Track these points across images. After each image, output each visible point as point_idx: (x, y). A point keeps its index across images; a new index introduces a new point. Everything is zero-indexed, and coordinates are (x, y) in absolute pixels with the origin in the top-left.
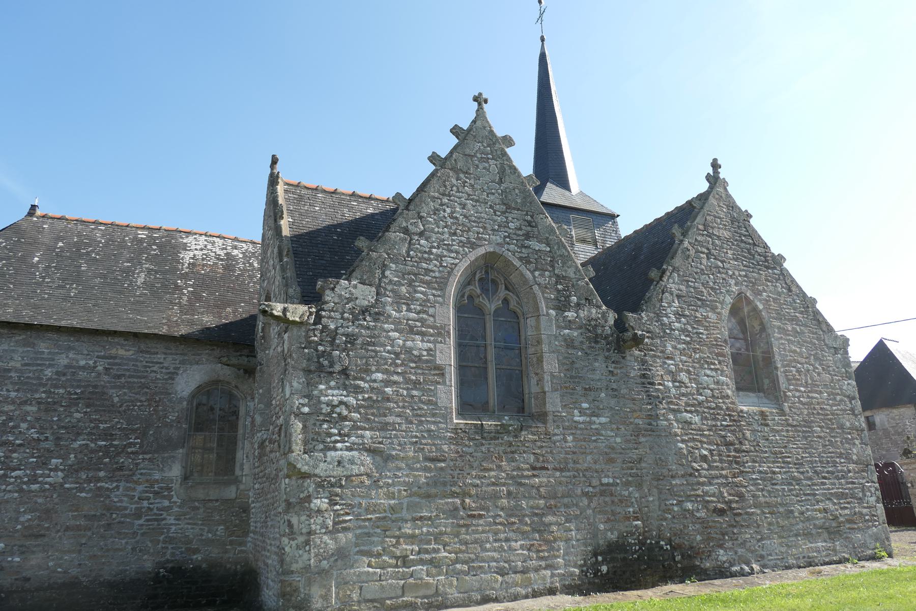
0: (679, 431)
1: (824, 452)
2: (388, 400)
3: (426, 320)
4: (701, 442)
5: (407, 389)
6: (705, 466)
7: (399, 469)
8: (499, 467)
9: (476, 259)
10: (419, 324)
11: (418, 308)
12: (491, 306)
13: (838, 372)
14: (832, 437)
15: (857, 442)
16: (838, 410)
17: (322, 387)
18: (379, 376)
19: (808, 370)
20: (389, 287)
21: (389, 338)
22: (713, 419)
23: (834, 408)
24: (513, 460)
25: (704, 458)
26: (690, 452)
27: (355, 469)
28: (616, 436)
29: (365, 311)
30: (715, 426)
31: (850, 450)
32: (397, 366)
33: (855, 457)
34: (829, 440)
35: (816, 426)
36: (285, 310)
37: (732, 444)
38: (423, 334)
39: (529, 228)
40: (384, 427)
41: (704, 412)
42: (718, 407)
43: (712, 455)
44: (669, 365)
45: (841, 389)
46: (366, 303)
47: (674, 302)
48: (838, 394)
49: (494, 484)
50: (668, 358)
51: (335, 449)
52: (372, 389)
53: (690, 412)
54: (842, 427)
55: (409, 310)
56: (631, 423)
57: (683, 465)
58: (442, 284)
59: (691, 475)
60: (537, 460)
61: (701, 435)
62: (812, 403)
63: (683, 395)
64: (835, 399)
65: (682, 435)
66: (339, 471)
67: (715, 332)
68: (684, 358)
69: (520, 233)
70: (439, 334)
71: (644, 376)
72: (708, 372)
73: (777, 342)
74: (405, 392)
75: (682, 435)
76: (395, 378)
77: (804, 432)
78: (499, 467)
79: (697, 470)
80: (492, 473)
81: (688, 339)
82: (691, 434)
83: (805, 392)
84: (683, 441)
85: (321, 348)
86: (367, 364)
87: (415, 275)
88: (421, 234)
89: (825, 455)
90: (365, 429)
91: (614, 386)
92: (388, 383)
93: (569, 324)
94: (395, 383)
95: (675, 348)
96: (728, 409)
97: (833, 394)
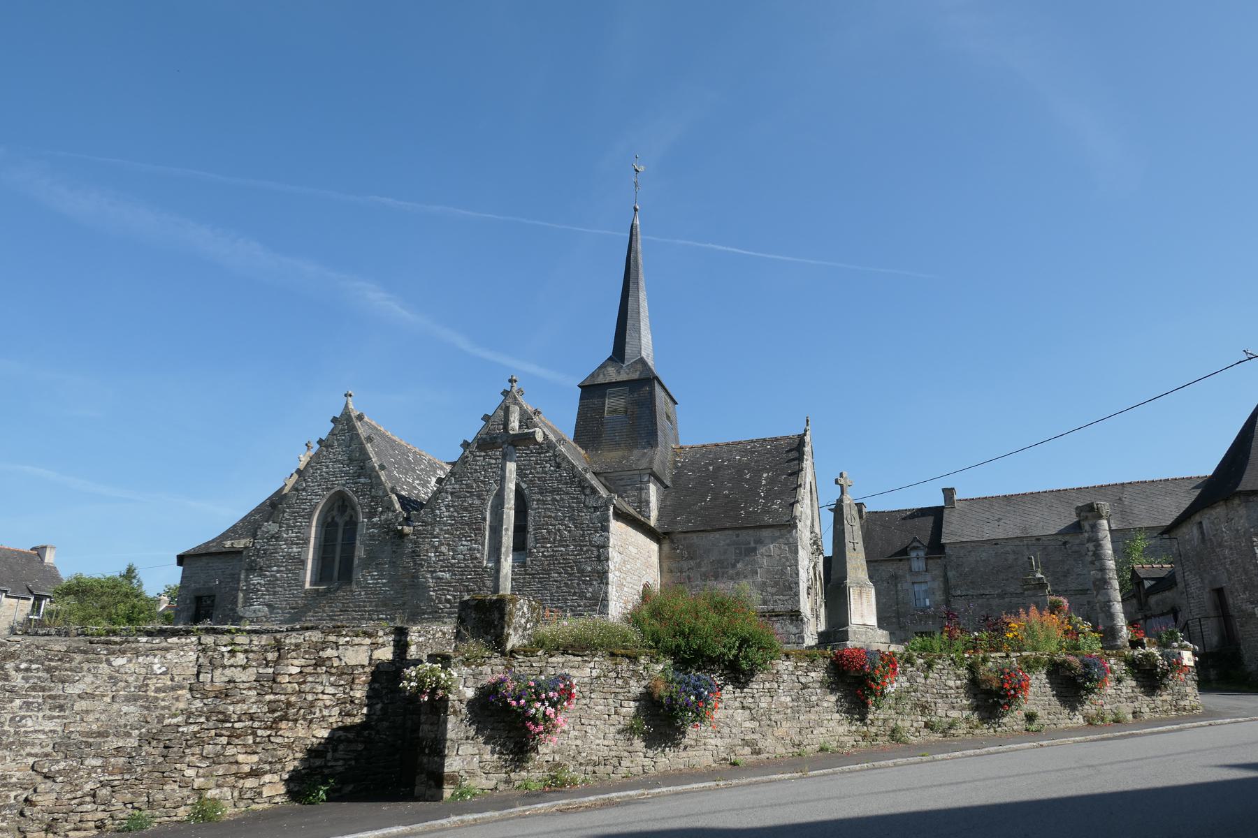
0: (431, 585)
1: (557, 592)
2: (277, 580)
3: (299, 536)
4: (448, 591)
5: (287, 574)
6: (448, 605)
7: (278, 613)
8: (324, 611)
9: (330, 497)
10: (295, 539)
11: (297, 531)
12: (340, 521)
13: (591, 527)
14: (569, 580)
15: (595, 583)
17: (251, 576)
18: (275, 568)
19: (559, 530)
20: (285, 522)
21: (281, 548)
22: (461, 575)
24: (331, 607)
25: (448, 601)
26: (437, 597)
27: (260, 614)
28: (391, 590)
29: (273, 537)
30: (463, 579)
32: (283, 562)
33: (589, 595)
34: (565, 583)
36: (232, 544)
37: (473, 590)
38: (297, 544)
39: (361, 471)
40: (275, 593)
41: (455, 571)
43: (455, 599)
44: (434, 542)
45: (590, 541)
46: (274, 532)
47: (447, 498)
48: (586, 545)
49: (320, 620)
50: (435, 538)
51: (254, 605)
52: (272, 575)
53: (444, 571)
54: (582, 571)
55: (292, 533)
56: (401, 582)
57: (431, 606)
58: (310, 515)
59: (436, 612)
60: (343, 606)
61: (449, 586)
63: (440, 560)
64: (581, 550)
65: (434, 587)
66: (254, 615)
67: (476, 513)
68: (447, 536)
69: (356, 475)
70: (305, 543)
71: (414, 552)
72: (464, 543)
73: (533, 513)
74: (285, 576)
75: (434, 587)
76: (282, 569)
77: (541, 578)
78: (324, 611)
79: (441, 609)
80: (320, 614)
81: (453, 522)
82: (441, 586)
83: (551, 547)
84: (434, 591)
85: (253, 558)
86: (270, 563)
87: (297, 513)
88: (304, 490)
89: (557, 595)
90: (266, 595)
91: (394, 560)
92: (278, 572)
93: (374, 525)
94: (282, 571)
95: (441, 530)
96: (474, 567)
97: (580, 546)
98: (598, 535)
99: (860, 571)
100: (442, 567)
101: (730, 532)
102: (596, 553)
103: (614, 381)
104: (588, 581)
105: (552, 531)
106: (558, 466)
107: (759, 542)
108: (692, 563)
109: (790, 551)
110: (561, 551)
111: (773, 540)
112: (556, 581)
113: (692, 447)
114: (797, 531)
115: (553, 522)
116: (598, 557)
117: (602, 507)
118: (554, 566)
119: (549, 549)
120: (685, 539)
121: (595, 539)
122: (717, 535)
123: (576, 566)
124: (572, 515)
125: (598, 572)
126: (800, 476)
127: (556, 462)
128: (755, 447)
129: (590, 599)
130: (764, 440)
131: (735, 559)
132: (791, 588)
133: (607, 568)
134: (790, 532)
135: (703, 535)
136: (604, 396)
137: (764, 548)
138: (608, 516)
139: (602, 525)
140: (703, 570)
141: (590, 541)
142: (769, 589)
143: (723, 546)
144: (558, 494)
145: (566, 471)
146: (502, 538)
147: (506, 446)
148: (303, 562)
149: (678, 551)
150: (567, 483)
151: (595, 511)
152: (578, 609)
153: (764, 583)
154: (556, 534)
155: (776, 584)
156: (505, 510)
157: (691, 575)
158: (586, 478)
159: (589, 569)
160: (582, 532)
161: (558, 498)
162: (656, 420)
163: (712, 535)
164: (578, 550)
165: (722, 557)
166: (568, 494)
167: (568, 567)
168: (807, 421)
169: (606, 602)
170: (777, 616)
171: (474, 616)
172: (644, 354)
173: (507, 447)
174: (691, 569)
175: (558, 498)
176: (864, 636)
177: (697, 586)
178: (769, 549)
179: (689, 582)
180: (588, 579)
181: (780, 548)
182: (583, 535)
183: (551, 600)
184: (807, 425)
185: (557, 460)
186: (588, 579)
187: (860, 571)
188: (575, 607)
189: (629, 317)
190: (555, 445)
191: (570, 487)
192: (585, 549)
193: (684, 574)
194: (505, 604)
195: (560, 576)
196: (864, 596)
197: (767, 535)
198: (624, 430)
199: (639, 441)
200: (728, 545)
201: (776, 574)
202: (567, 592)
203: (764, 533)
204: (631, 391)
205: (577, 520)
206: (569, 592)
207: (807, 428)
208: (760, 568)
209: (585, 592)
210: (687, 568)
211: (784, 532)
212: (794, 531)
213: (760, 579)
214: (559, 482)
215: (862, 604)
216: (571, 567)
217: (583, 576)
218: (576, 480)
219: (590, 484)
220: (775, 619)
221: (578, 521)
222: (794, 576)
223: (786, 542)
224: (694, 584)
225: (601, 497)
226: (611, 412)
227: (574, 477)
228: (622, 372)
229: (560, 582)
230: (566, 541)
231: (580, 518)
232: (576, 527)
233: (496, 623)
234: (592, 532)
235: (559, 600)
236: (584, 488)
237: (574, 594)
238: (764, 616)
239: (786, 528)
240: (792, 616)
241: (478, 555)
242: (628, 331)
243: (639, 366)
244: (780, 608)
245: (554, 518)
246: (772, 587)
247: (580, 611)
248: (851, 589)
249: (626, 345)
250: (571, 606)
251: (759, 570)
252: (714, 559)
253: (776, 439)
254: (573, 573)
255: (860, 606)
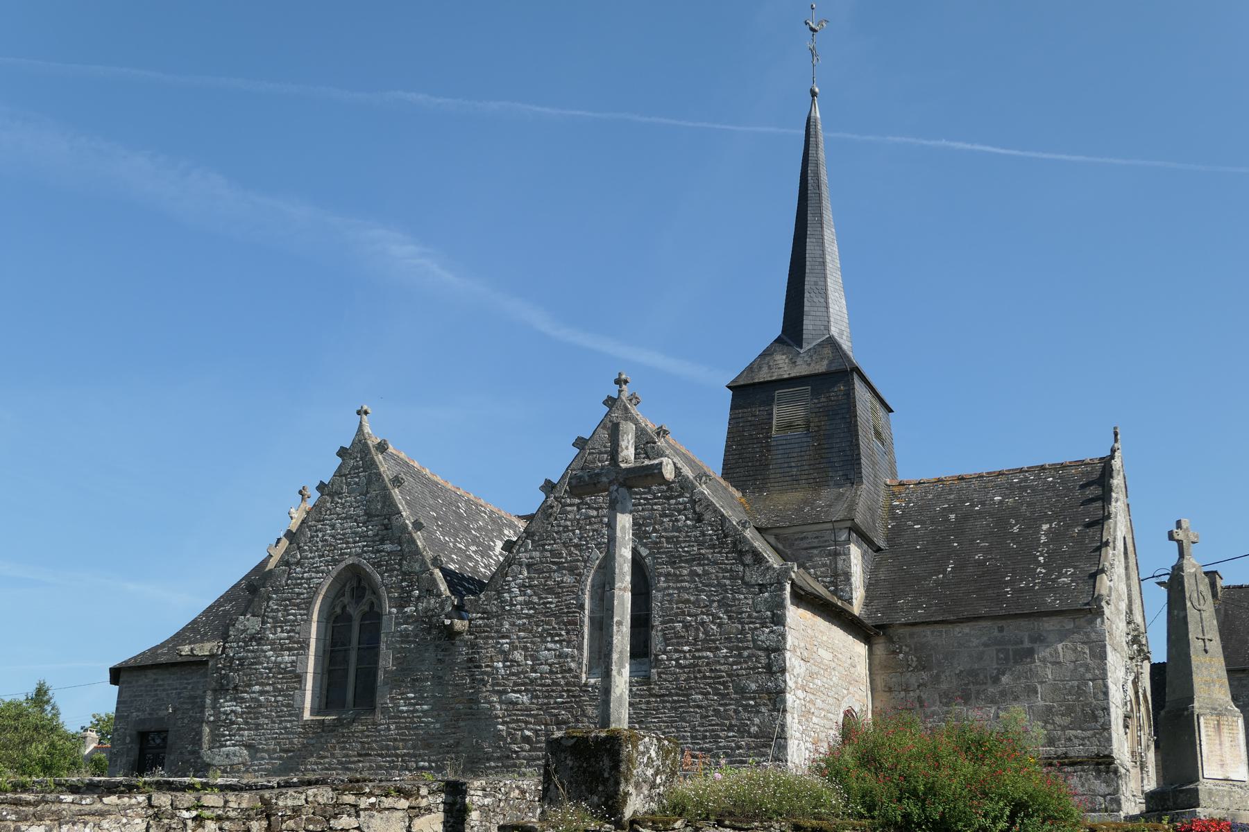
0: (499, 713)
1: (702, 725)
2: (261, 706)
3: (293, 637)
4: (527, 723)
5: (275, 696)
6: (527, 747)
7: (263, 759)
8: (333, 756)
9: (339, 574)
10: (287, 641)
11: (288, 628)
12: (355, 612)
13: (756, 618)
14: (721, 705)
15: (763, 709)
16: (741, 669)
17: (222, 701)
18: (257, 688)
19: (703, 623)
20: (271, 614)
21: (265, 656)
22: (546, 697)
23: (735, 667)
24: (343, 748)
25: (526, 739)
26: (509, 734)
27: (236, 760)
28: (437, 722)
29: (253, 638)
30: (549, 704)
31: (749, 720)
32: (268, 678)
33: (754, 729)
34: (714, 710)
35: (696, 693)
36: (192, 650)
37: (565, 722)
38: (289, 649)
39: (385, 532)
40: (258, 727)
41: (536, 691)
42: (555, 684)
43: (537, 735)
44: (502, 644)
45: (754, 641)
46: (254, 631)
47: (521, 573)
48: (748, 648)
49: (327, 769)
50: (503, 637)
51: (225, 746)
52: (252, 698)
53: (519, 692)
54: (742, 691)
55: (282, 631)
56: (452, 709)
57: (500, 747)
58: (309, 604)
59: (508, 757)
60: (363, 748)
61: (527, 715)
62: (697, 665)
63: (513, 674)
64: (740, 655)
65: (504, 716)
66: (226, 762)
67: (568, 598)
68: (522, 634)
69: (377, 538)
70: (302, 648)
71: (470, 660)
72: (549, 645)
73: (659, 595)
74: (273, 699)
75: (504, 716)
76: (268, 688)
77: (674, 702)
78: (333, 756)
79: (516, 752)
80: (327, 760)
81: (532, 612)
82: (515, 715)
83: (690, 651)
84: (503, 723)
85: (223, 672)
86: (250, 680)
87: (289, 600)
88: (298, 563)
89: (702, 729)
90: (245, 730)
91: (440, 674)
92: (262, 693)
93: (407, 619)
94: (268, 692)
95: (513, 624)
96: (567, 684)
97: (738, 648)
98: (767, 630)
99: (1217, 686)
100: (516, 684)
101: (989, 623)
102: (764, 661)
103: (786, 376)
104: (752, 706)
105: (691, 625)
106: (699, 518)
107: (1039, 639)
108: (924, 675)
109: (1093, 655)
110: (707, 657)
111: (1063, 636)
112: (699, 707)
113: (920, 483)
114: (1103, 621)
115: (693, 611)
116: (768, 667)
117: (772, 585)
118: (696, 683)
119: (687, 655)
120: (911, 635)
121: (762, 638)
122: (966, 629)
123: (732, 681)
124: (723, 598)
125: (769, 692)
126: (1105, 527)
127: (695, 512)
128: (1026, 479)
129: (756, 736)
130: (1042, 468)
131: (999, 669)
132: (1095, 718)
133: (783, 686)
134: (1092, 621)
135: (943, 628)
136: (769, 402)
137: (1048, 650)
138: (783, 600)
139: (774, 615)
140: (944, 686)
141: (754, 641)
142: (1057, 719)
143: (977, 647)
144: (699, 565)
145: (712, 525)
146: (612, 637)
147: (615, 487)
148: (300, 678)
149: (901, 656)
150: (713, 547)
151: (761, 592)
152: (737, 752)
153: (1049, 709)
154: (697, 629)
155: (1070, 710)
156: (617, 592)
157: (924, 696)
158: (744, 537)
159: (753, 686)
160: (740, 626)
161: (699, 570)
162: (857, 440)
163: (957, 629)
164: (735, 656)
165: (976, 666)
166: (715, 563)
167: (719, 683)
168: (1116, 434)
169: (782, 741)
170: (1073, 764)
171: (570, 763)
172: (834, 331)
173: (617, 490)
174: (924, 685)
175: (699, 570)
176: (1226, 799)
177: (933, 714)
178: (1056, 651)
179: (921, 707)
180: (752, 702)
181: (1075, 650)
182: (742, 632)
183: (692, 737)
184: (1116, 441)
185: (697, 509)
186: (752, 702)
187: (1217, 686)
188: (732, 749)
189: (807, 271)
190: (693, 484)
191: (720, 552)
192: (746, 653)
193: (912, 694)
194: (620, 745)
195: (708, 700)
196: (1225, 730)
197: (1052, 628)
198: (806, 458)
199: (831, 474)
200: (985, 645)
201: (1070, 693)
202: (717, 725)
203: (1046, 625)
204: (815, 393)
205: (732, 606)
206: (723, 725)
207: (1116, 445)
208: (1041, 683)
209: (747, 725)
210: (916, 684)
211: (1082, 622)
212: (1099, 620)
213: (1042, 703)
214: (701, 544)
215: (1220, 744)
216: (723, 684)
217: (744, 698)
218: (729, 540)
219: (752, 546)
220: (1069, 769)
221: (734, 608)
222: (1101, 696)
223: (1086, 640)
224: (929, 711)
225: (770, 568)
226: (780, 428)
227: (726, 536)
228: (799, 361)
229: (706, 708)
230: (714, 641)
231: (737, 602)
232: (730, 618)
233: (606, 775)
234: (758, 625)
235: (705, 737)
236: (741, 553)
237: (730, 728)
238: (1051, 765)
239: (1085, 616)
240: (1098, 764)
241: (573, 665)
242: (807, 295)
243: (827, 351)
244: (1077, 751)
245: (693, 603)
246: (1063, 715)
247: (740, 755)
248: (1202, 720)
249: (805, 317)
250: (725, 747)
251: (1039, 686)
252: (961, 668)
253: (1063, 466)
254: (728, 694)
255: (1219, 747)
